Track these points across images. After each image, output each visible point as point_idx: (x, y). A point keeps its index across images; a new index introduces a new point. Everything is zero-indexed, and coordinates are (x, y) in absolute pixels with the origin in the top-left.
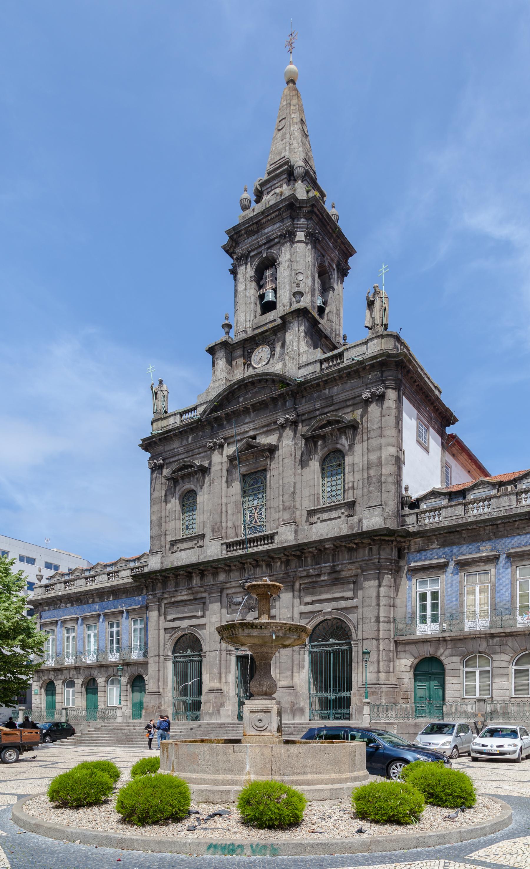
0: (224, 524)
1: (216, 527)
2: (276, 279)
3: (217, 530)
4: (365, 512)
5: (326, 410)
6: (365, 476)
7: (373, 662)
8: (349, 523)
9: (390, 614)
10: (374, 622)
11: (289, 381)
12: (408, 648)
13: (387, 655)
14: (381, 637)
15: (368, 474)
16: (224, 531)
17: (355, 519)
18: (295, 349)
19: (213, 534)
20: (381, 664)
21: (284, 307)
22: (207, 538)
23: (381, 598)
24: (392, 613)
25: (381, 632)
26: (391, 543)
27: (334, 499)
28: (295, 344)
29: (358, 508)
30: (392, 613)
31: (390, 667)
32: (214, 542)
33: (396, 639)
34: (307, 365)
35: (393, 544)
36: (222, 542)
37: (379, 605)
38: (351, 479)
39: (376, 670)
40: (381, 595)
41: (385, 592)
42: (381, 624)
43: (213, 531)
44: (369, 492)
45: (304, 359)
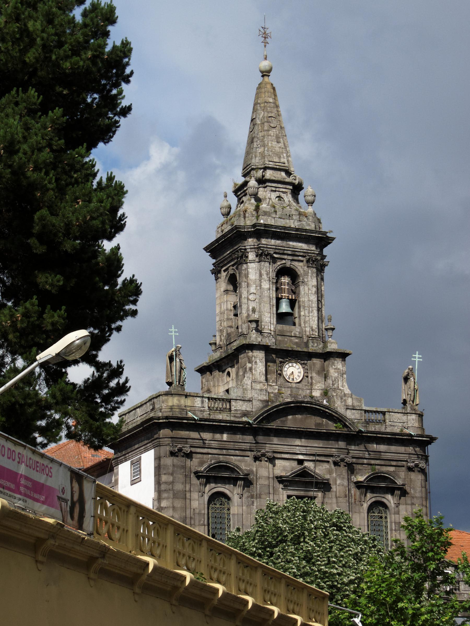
5: (373, 462)
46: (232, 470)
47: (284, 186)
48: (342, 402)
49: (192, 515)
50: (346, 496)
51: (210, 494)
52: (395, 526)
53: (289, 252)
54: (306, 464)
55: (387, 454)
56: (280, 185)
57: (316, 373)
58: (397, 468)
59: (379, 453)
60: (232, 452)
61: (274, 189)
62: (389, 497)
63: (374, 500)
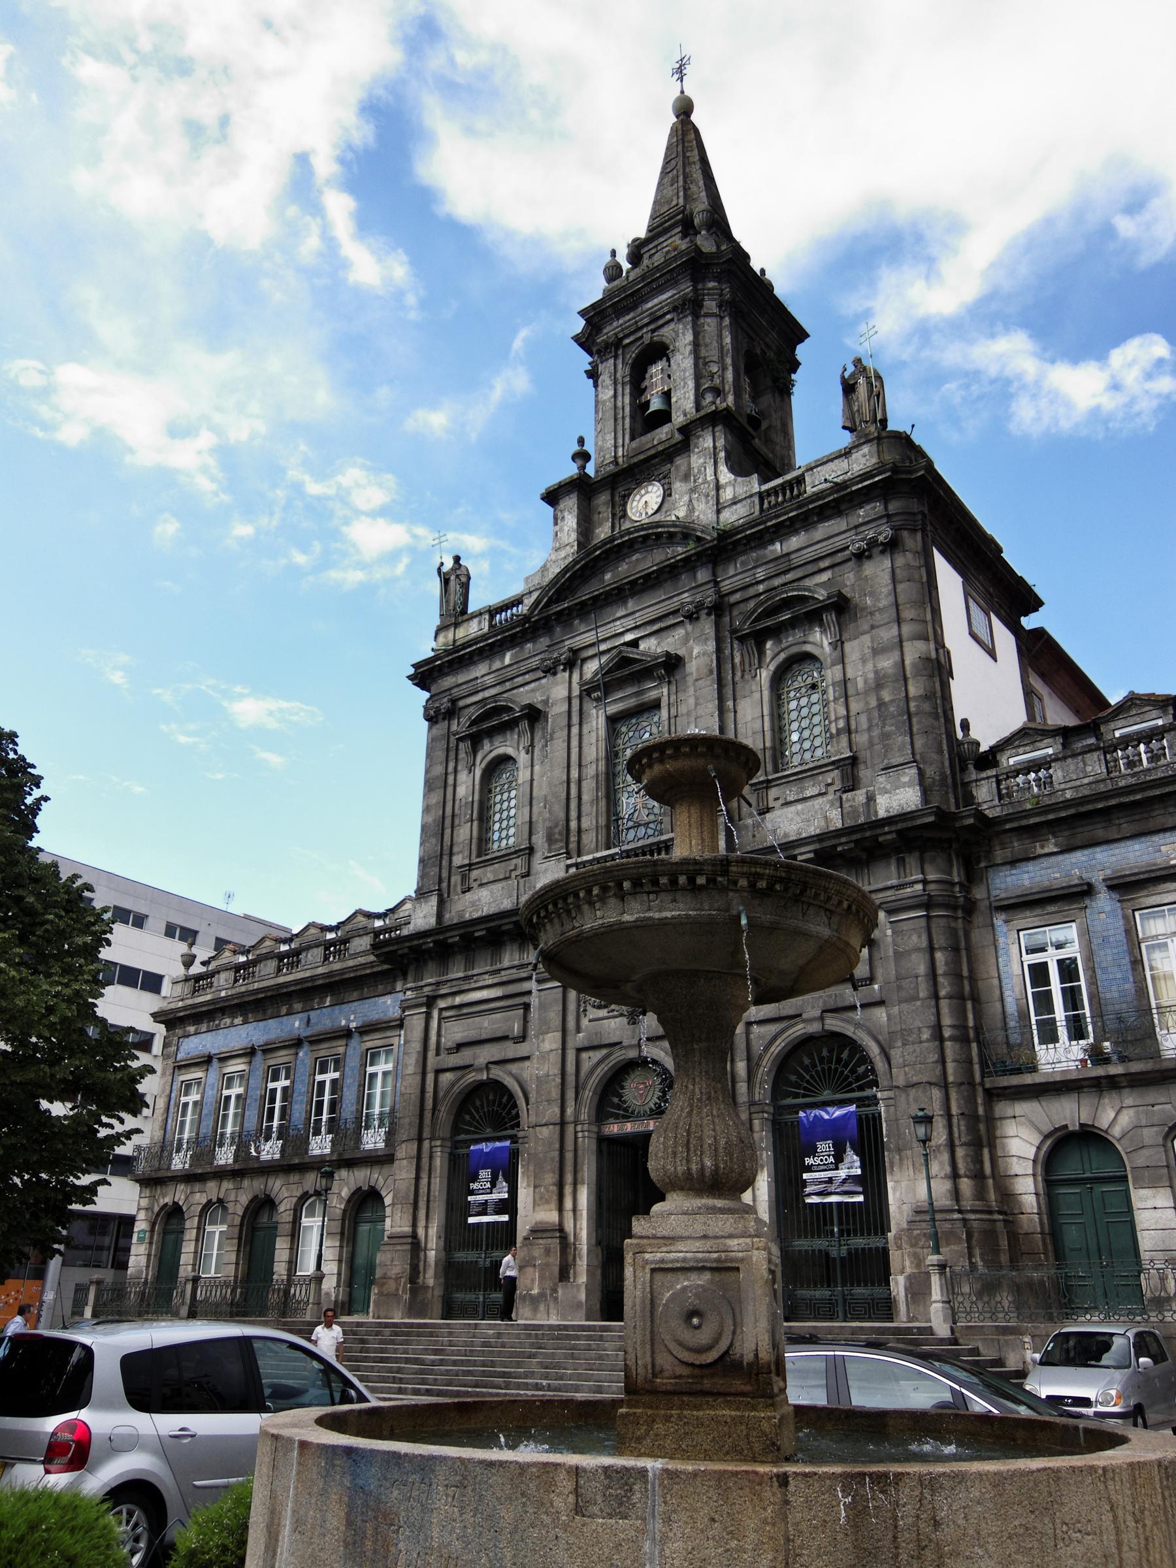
0: (573, 824)
1: (557, 830)
2: (669, 376)
3: (557, 836)
4: (881, 779)
6: (873, 703)
7: (938, 1147)
8: (846, 805)
9: (966, 1019)
10: (928, 1041)
11: (702, 532)
12: (1022, 1108)
13: (973, 1128)
14: (951, 1079)
15: (879, 699)
16: (573, 838)
17: (860, 796)
18: (709, 479)
19: (550, 845)
20: (960, 1152)
21: (685, 415)
22: (538, 857)
23: (941, 979)
24: (970, 1016)
25: (951, 1067)
26: (946, 845)
27: (808, 756)
28: (710, 471)
29: (864, 773)
30: (970, 1016)
31: (981, 1163)
32: (552, 863)
33: (988, 1086)
34: (735, 503)
35: (951, 847)
36: (569, 862)
37: (936, 997)
38: (842, 711)
39: (948, 1169)
40: (940, 971)
41: (946, 964)
42: (948, 1044)
43: (550, 840)
44: (885, 736)
45: (727, 494)
46: (508, 709)
47: (669, 235)
48: (707, 503)
49: (456, 811)
50: (711, 672)
51: (483, 765)
52: (834, 692)
53: (646, 321)
54: (643, 646)
55: (805, 551)
56: (661, 239)
57: (681, 481)
58: (836, 569)
59: (786, 559)
60: (520, 680)
61: (653, 251)
62: (817, 635)
63: (782, 656)
